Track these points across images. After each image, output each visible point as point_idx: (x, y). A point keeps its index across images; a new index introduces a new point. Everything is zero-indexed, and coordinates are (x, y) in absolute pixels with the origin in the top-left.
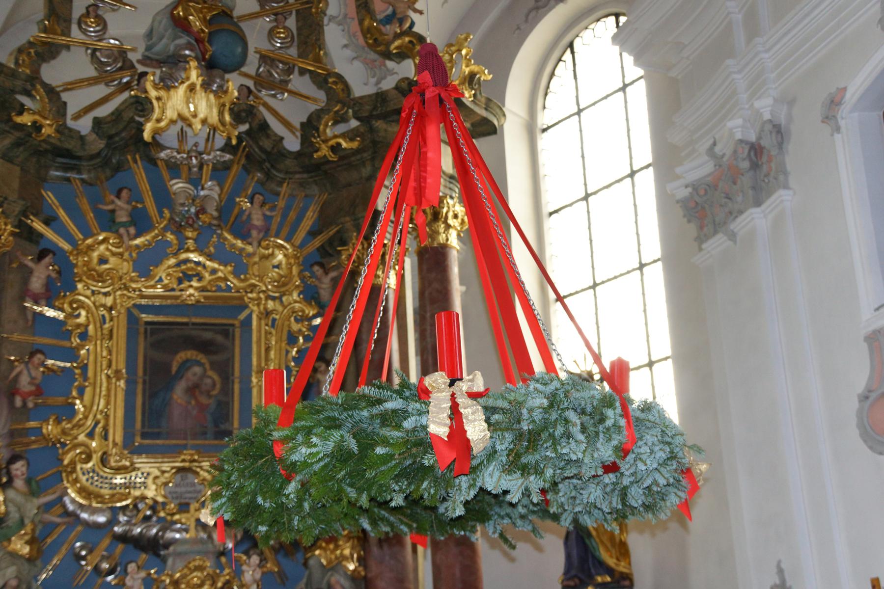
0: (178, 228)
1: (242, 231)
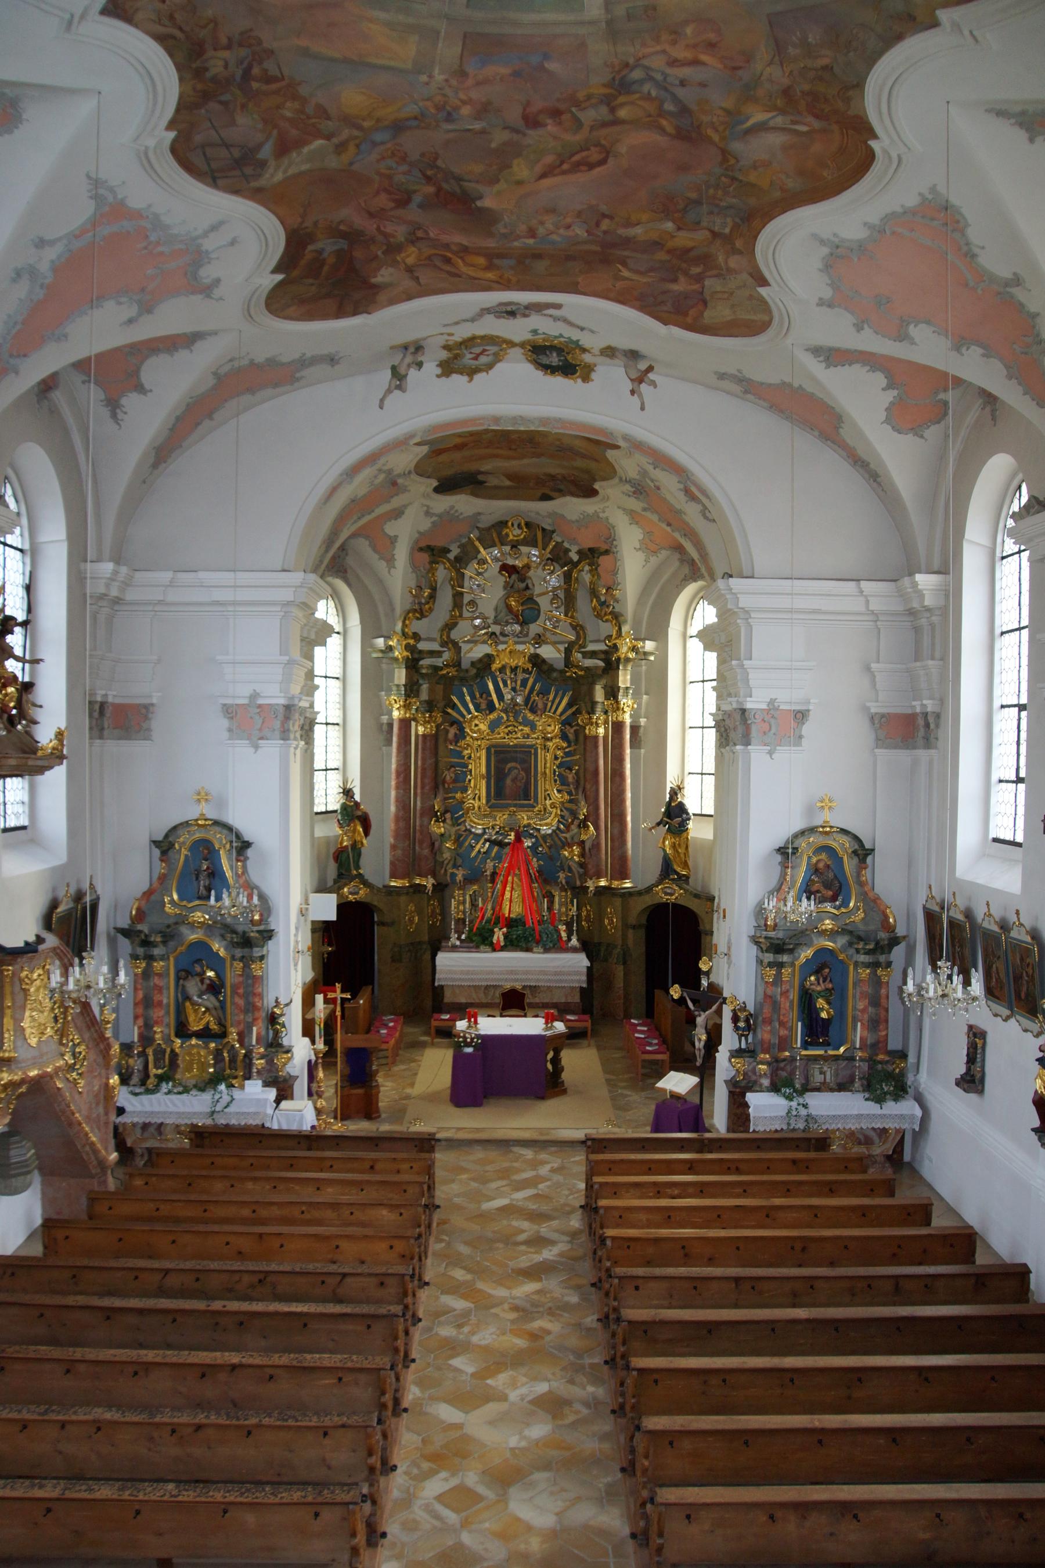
0: (505, 711)
1: (533, 711)
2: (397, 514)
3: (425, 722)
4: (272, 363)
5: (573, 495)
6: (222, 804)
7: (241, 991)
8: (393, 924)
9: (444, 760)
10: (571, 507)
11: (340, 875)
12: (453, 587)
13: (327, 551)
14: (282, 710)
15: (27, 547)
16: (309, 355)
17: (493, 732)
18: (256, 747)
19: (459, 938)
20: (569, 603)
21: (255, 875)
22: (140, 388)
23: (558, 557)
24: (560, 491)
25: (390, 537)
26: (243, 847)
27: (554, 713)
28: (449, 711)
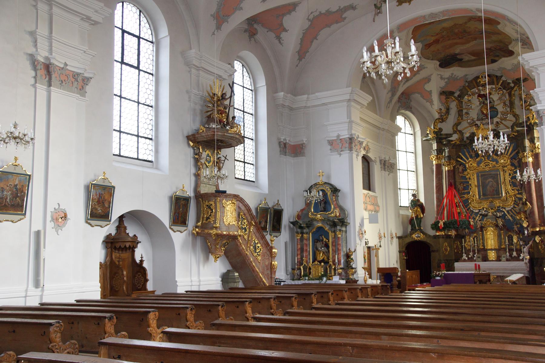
2: (428, 80)
3: (448, 165)
4: (328, 12)
5: (504, 56)
6: (329, 177)
7: (334, 244)
8: (437, 251)
9: (458, 180)
10: (506, 63)
11: (412, 230)
12: (458, 108)
13: (393, 95)
14: (348, 139)
15: (253, 89)
16: (342, 7)
17: (479, 166)
18: (340, 155)
19: (467, 256)
20: (512, 105)
21: (341, 203)
22: (285, 30)
23: (505, 86)
24: (498, 56)
25: (429, 92)
26: (335, 190)
27: (507, 154)
28: (459, 160)
